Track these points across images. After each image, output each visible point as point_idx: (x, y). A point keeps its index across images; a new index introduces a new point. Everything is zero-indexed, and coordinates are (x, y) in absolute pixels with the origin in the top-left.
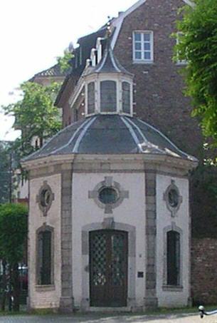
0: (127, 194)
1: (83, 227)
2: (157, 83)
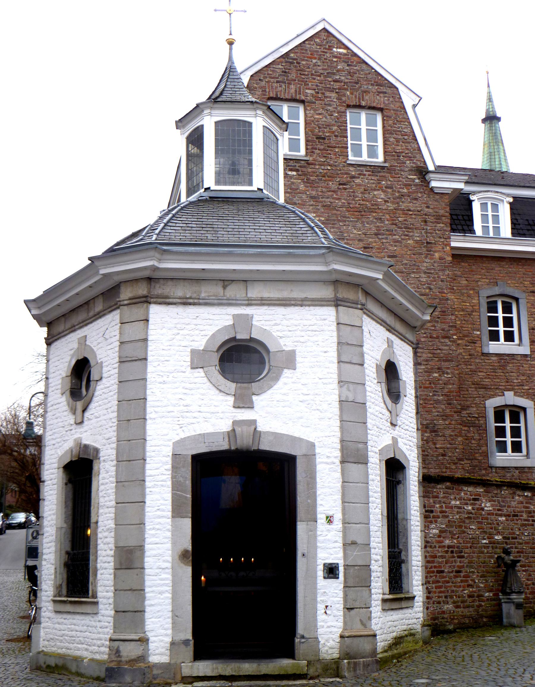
0: (290, 360)
1: (176, 444)
2: (314, 193)
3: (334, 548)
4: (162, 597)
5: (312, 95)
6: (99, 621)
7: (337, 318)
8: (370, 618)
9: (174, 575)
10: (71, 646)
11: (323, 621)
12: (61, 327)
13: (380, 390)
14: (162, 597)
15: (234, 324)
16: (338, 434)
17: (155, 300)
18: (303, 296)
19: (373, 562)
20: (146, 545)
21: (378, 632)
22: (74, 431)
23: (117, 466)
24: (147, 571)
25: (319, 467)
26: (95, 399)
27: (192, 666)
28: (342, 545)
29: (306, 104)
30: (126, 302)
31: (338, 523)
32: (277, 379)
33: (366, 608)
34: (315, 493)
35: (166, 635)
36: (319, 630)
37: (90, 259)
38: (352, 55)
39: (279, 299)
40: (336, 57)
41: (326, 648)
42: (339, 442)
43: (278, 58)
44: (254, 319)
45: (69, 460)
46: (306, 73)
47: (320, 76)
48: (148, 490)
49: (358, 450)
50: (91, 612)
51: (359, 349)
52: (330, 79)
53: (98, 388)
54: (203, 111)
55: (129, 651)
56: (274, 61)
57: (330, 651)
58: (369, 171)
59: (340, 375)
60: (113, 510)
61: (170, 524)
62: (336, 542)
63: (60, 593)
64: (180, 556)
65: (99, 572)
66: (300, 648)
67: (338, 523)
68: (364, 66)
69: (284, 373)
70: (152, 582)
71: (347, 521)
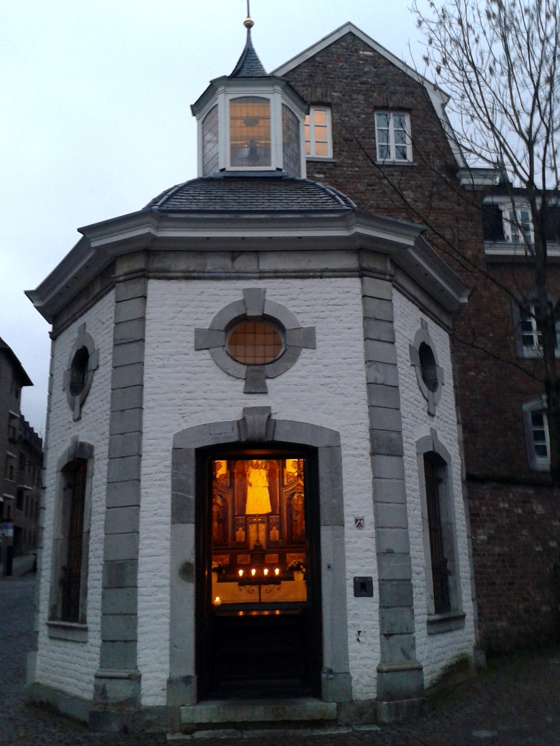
0: (309, 339)
1: (177, 436)
3: (366, 558)
4: (158, 622)
5: (339, 98)
6: (88, 652)
7: (363, 290)
8: (413, 647)
9: (173, 595)
10: (64, 679)
11: (355, 651)
12: (65, 318)
13: (414, 374)
14: (158, 622)
15: (244, 300)
16: (367, 421)
17: (153, 274)
18: (323, 266)
19: (414, 575)
20: (139, 558)
21: (423, 664)
22: (73, 429)
23: (109, 464)
24: (140, 590)
25: (345, 461)
26: (92, 391)
27: (194, 710)
28: (375, 554)
29: (333, 106)
30: (121, 278)
31: (369, 527)
32: (294, 360)
33: (408, 634)
34: (341, 491)
35: (163, 671)
36: (350, 663)
37: (80, 230)
38: (379, 58)
39: (295, 271)
40: (363, 59)
41: (360, 686)
42: (367, 430)
43: (304, 62)
44: (267, 294)
45: (66, 462)
46: (333, 76)
47: (346, 79)
48: (143, 491)
49: (390, 440)
50: (80, 640)
51: (388, 325)
52: (357, 82)
53: (95, 378)
54: (217, 89)
55: (119, 691)
56: (299, 65)
57: (365, 690)
58: (397, 171)
59: (367, 354)
60: (103, 516)
61: (169, 531)
62: (368, 550)
63: (54, 616)
64: (180, 571)
65: (89, 592)
66: (329, 686)
67: (369, 527)
68: (391, 67)
69: (301, 353)
70: (146, 603)
71: (380, 524)
